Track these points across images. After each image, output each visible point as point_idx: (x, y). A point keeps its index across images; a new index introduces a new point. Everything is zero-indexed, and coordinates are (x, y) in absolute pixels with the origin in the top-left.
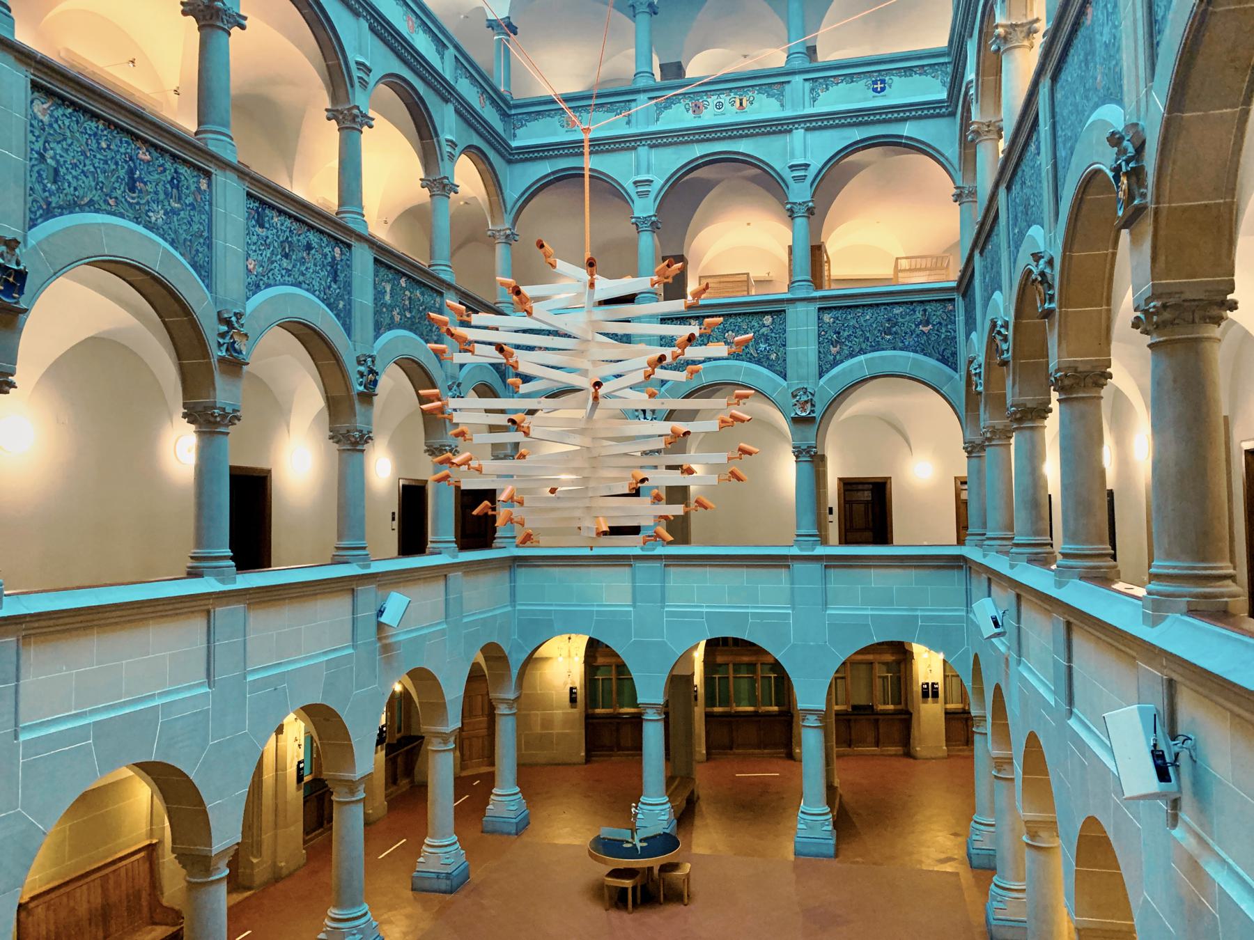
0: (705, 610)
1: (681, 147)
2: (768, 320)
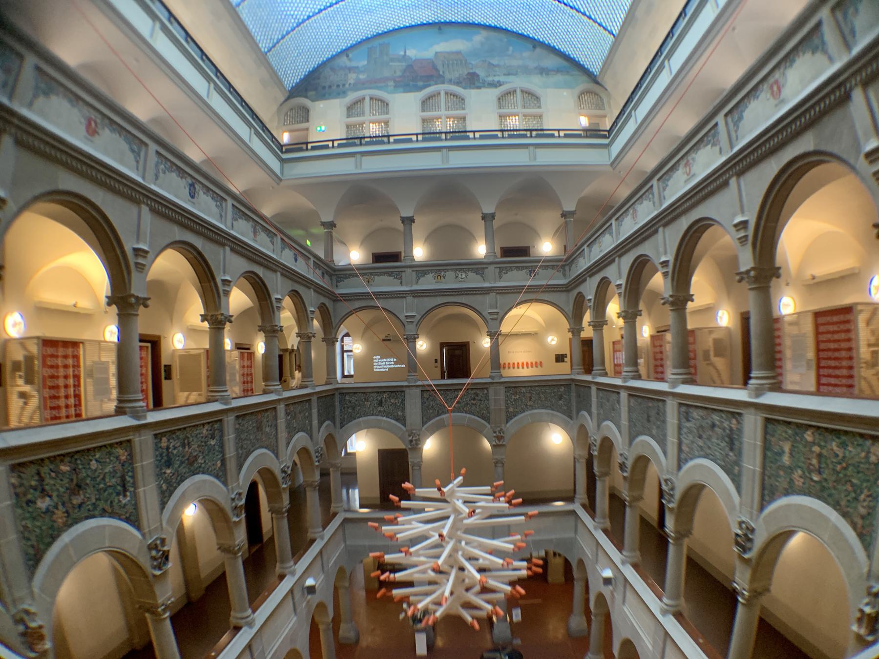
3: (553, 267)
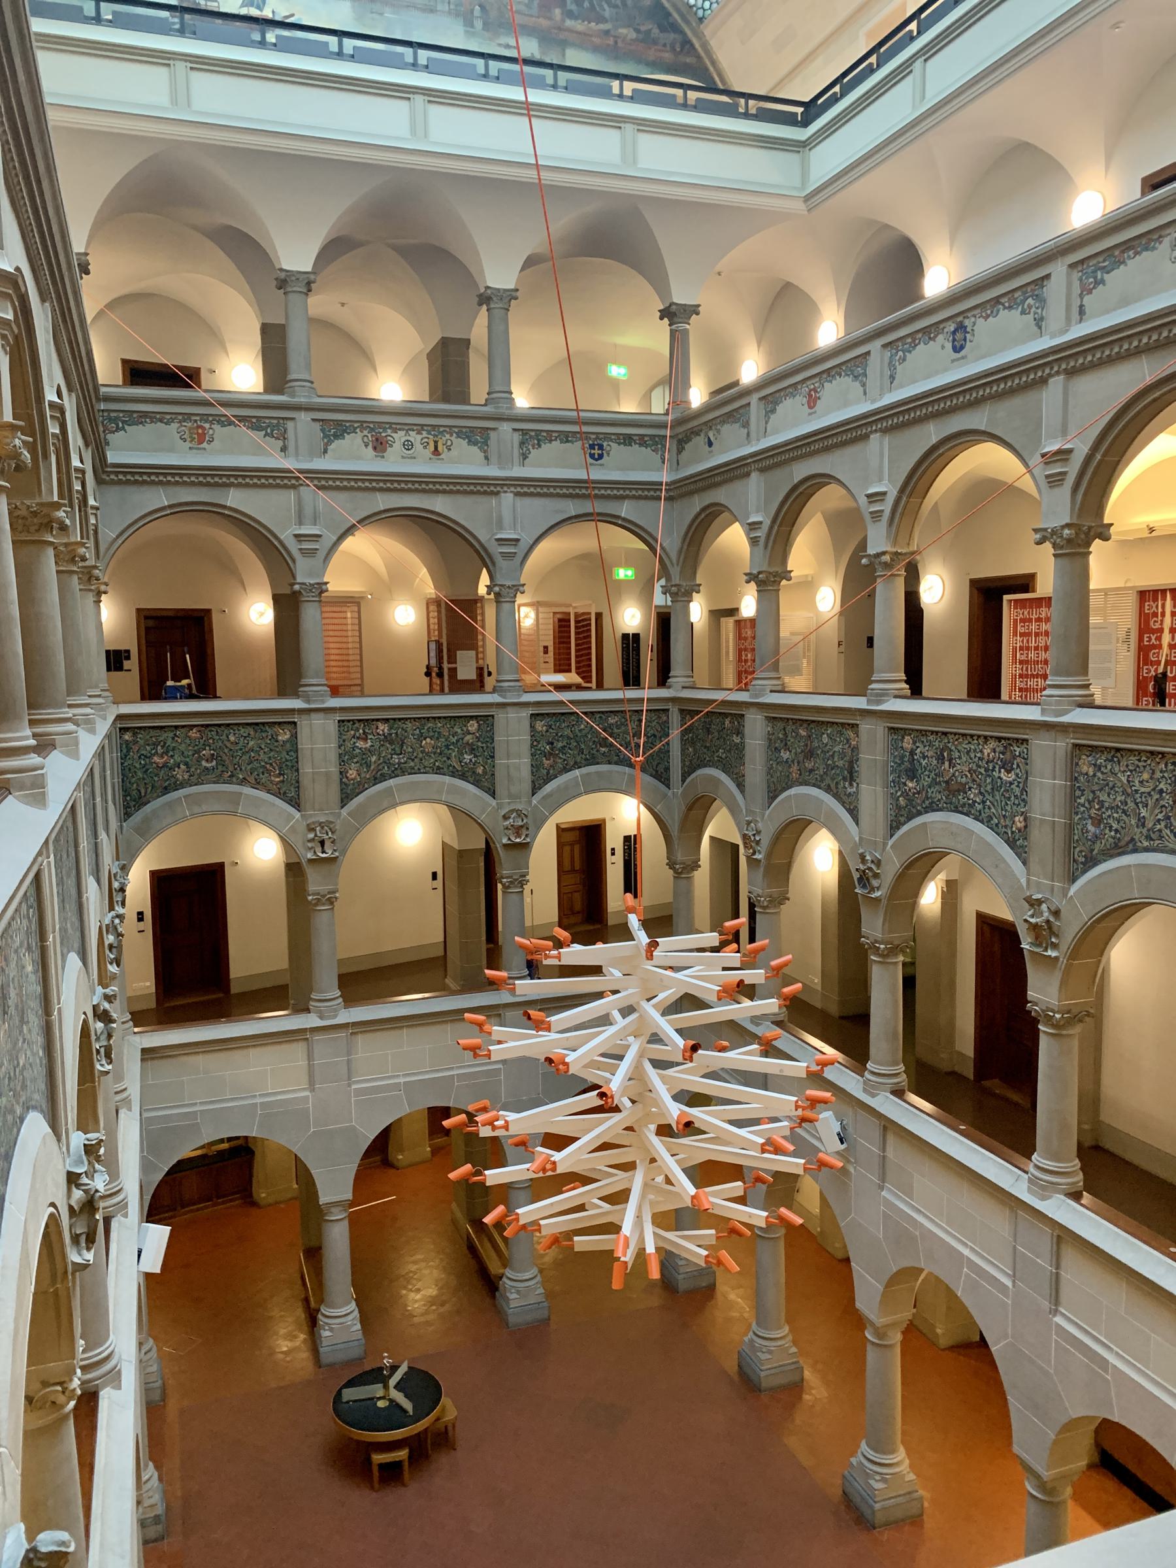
0: (402, 1080)
1: (359, 494)
2: (473, 726)
3: (642, 441)
